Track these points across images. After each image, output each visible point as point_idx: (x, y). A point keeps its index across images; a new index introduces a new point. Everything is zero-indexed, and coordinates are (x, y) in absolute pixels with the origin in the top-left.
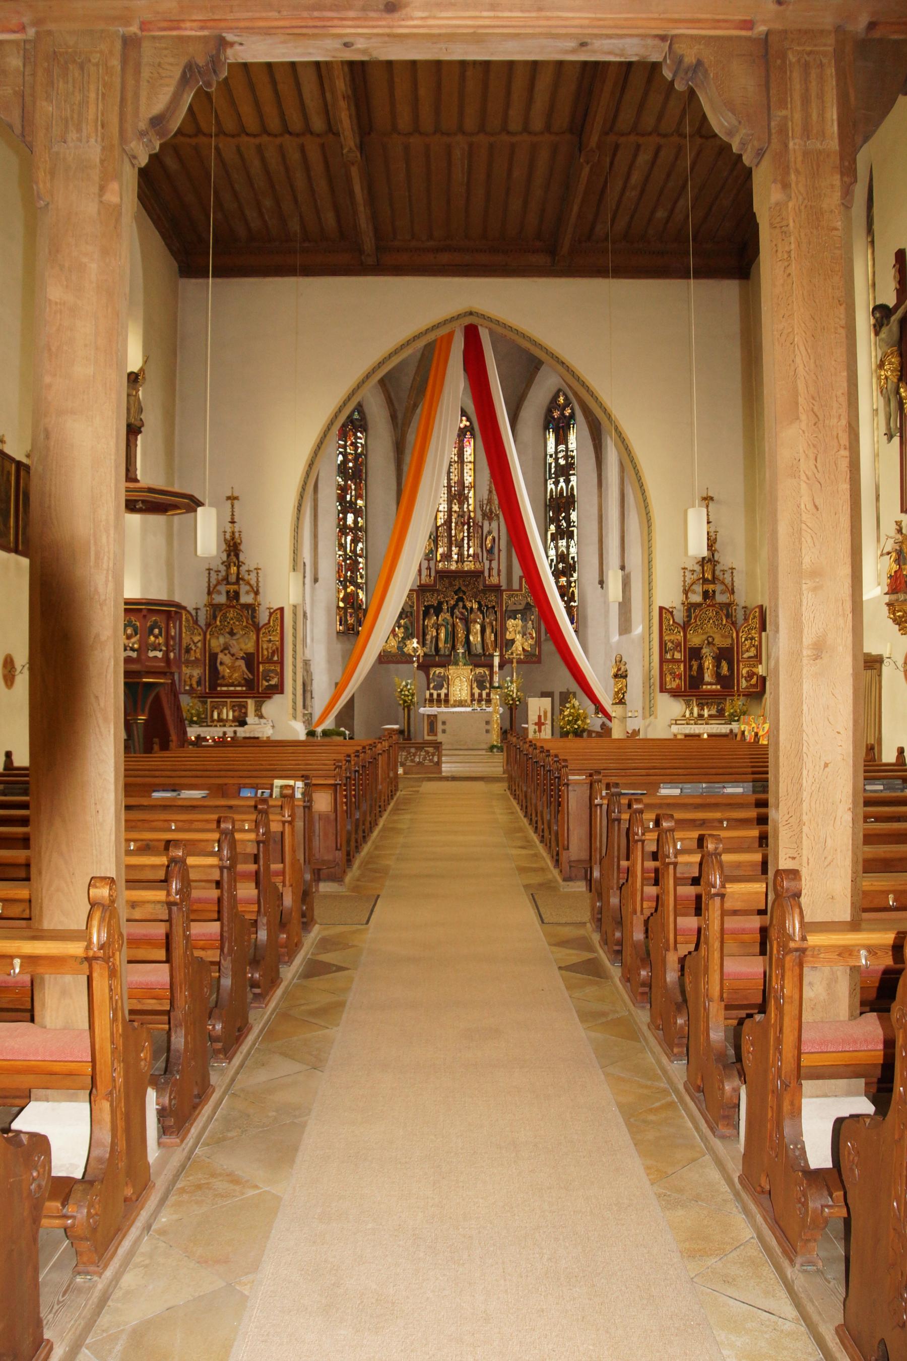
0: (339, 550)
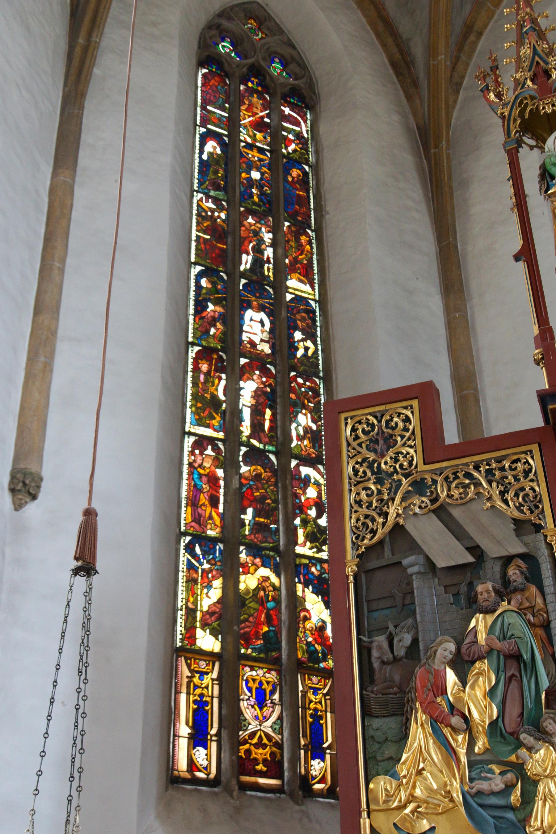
0: (200, 422)
